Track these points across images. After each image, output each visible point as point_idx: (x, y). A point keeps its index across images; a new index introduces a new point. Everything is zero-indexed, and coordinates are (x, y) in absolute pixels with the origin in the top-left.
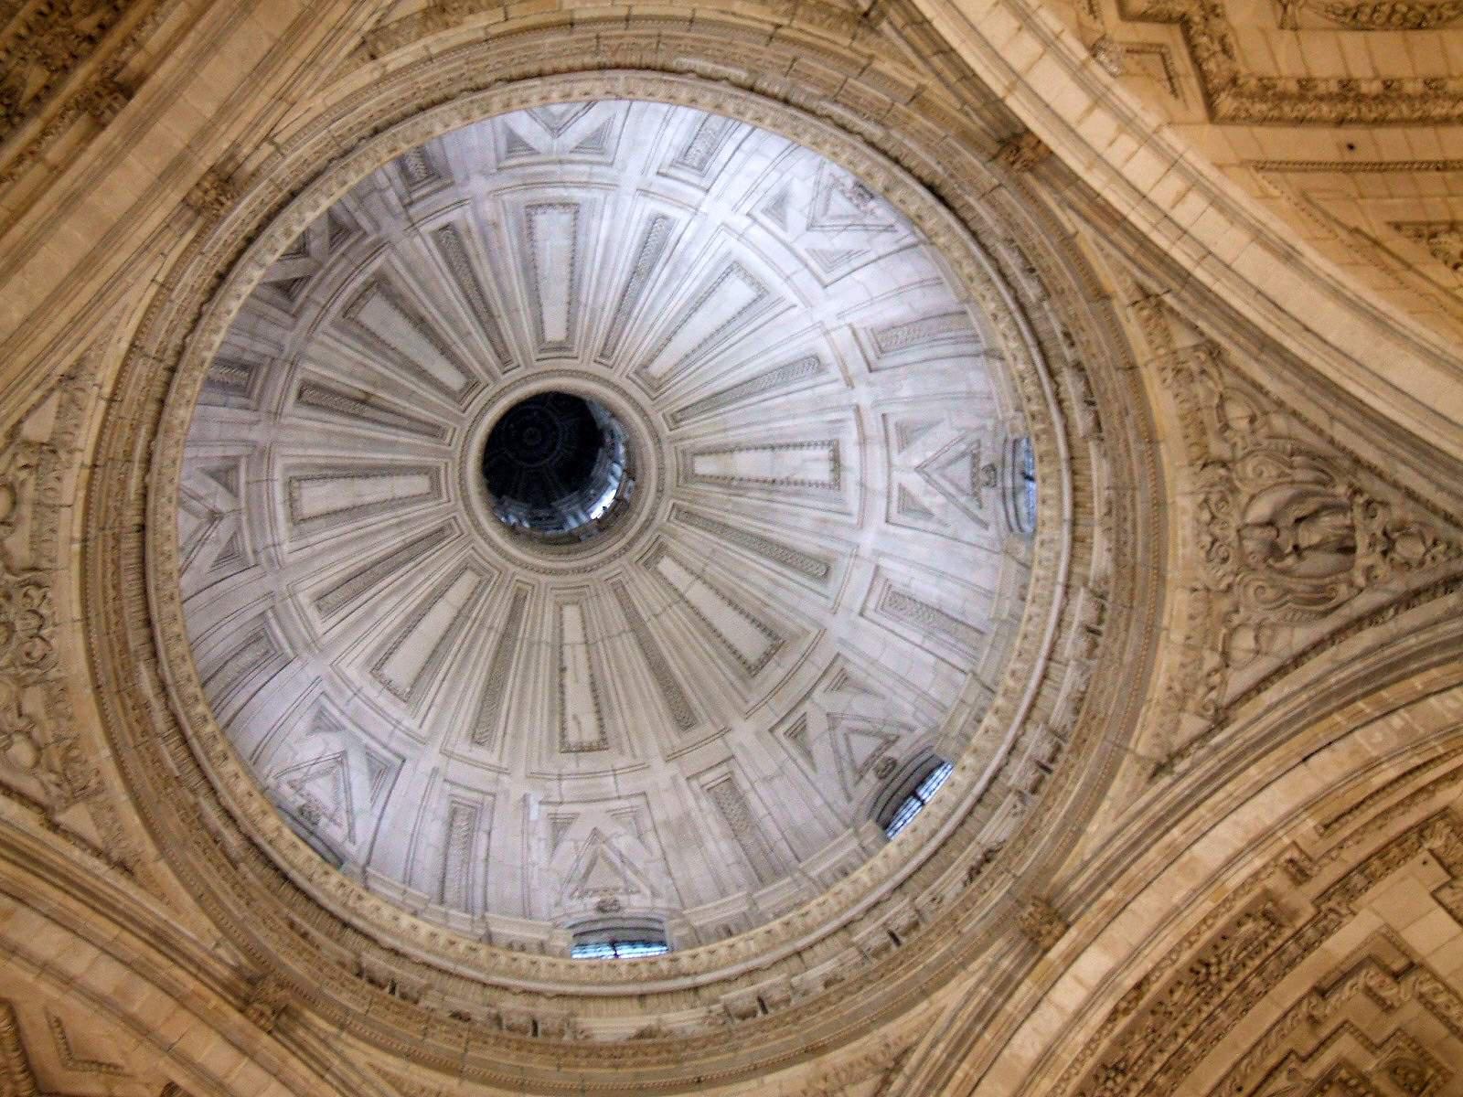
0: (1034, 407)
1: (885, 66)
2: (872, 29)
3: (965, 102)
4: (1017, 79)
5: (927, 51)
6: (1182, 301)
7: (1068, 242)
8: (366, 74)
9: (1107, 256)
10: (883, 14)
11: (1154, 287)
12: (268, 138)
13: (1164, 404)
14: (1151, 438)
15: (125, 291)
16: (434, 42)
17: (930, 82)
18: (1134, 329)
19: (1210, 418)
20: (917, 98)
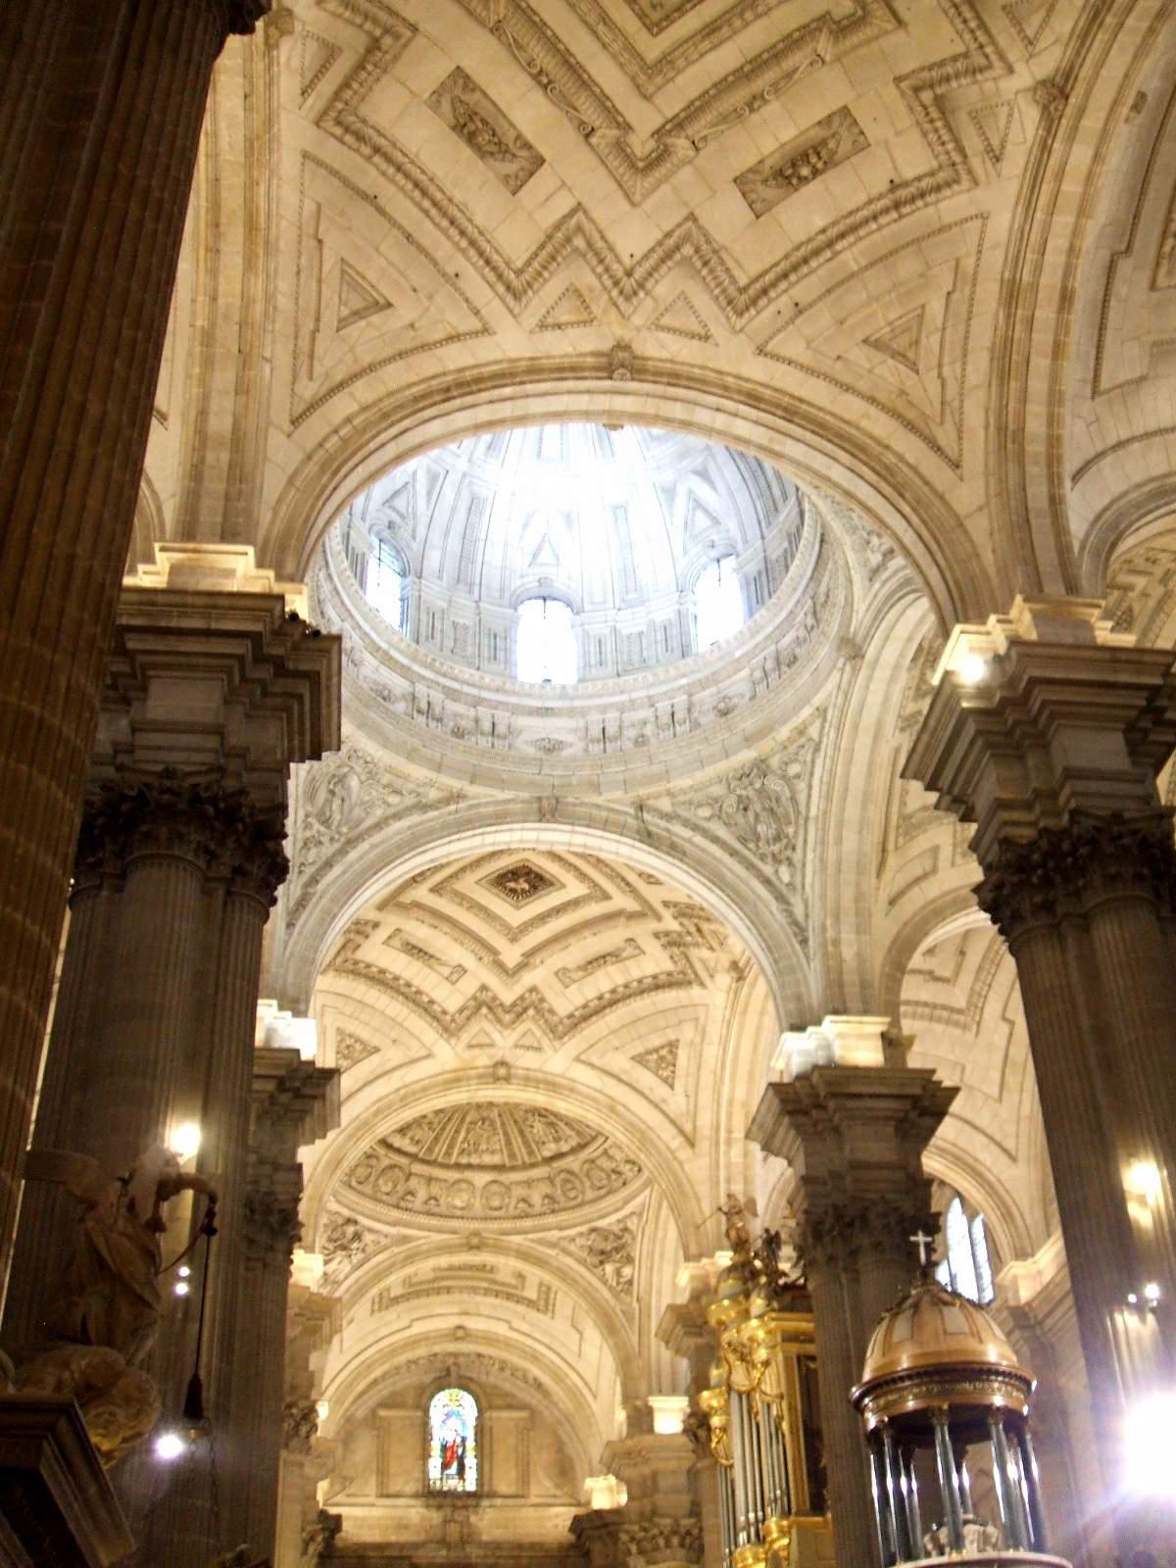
0: (437, 664)
1: (618, 794)
2: (633, 803)
3: (582, 804)
4: (573, 832)
5: (612, 816)
6: (450, 814)
7: (502, 784)
8: (818, 700)
9: (485, 796)
10: (636, 818)
11: (462, 805)
12: (842, 670)
13: (419, 772)
14: (411, 755)
15: (867, 610)
16: (796, 721)
17: (599, 800)
18: (456, 784)
19: (398, 783)
20: (596, 787)
